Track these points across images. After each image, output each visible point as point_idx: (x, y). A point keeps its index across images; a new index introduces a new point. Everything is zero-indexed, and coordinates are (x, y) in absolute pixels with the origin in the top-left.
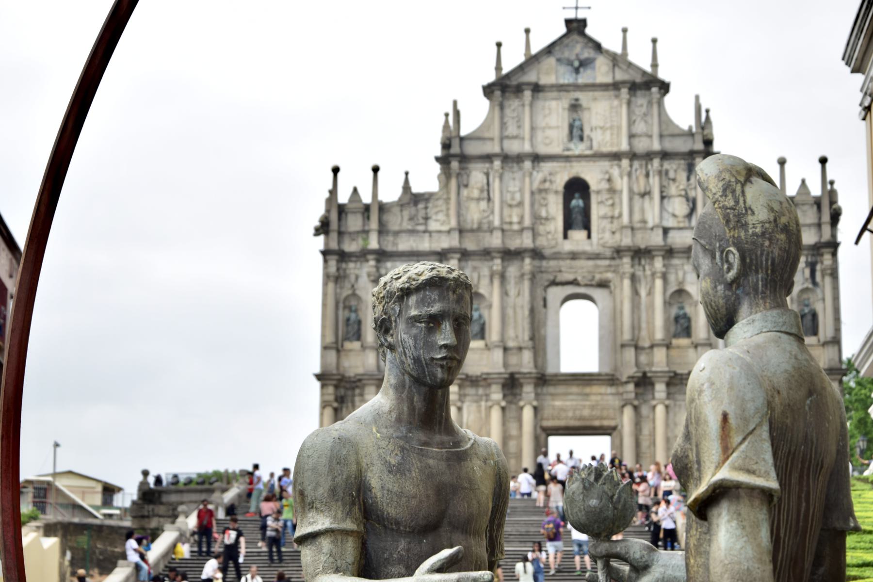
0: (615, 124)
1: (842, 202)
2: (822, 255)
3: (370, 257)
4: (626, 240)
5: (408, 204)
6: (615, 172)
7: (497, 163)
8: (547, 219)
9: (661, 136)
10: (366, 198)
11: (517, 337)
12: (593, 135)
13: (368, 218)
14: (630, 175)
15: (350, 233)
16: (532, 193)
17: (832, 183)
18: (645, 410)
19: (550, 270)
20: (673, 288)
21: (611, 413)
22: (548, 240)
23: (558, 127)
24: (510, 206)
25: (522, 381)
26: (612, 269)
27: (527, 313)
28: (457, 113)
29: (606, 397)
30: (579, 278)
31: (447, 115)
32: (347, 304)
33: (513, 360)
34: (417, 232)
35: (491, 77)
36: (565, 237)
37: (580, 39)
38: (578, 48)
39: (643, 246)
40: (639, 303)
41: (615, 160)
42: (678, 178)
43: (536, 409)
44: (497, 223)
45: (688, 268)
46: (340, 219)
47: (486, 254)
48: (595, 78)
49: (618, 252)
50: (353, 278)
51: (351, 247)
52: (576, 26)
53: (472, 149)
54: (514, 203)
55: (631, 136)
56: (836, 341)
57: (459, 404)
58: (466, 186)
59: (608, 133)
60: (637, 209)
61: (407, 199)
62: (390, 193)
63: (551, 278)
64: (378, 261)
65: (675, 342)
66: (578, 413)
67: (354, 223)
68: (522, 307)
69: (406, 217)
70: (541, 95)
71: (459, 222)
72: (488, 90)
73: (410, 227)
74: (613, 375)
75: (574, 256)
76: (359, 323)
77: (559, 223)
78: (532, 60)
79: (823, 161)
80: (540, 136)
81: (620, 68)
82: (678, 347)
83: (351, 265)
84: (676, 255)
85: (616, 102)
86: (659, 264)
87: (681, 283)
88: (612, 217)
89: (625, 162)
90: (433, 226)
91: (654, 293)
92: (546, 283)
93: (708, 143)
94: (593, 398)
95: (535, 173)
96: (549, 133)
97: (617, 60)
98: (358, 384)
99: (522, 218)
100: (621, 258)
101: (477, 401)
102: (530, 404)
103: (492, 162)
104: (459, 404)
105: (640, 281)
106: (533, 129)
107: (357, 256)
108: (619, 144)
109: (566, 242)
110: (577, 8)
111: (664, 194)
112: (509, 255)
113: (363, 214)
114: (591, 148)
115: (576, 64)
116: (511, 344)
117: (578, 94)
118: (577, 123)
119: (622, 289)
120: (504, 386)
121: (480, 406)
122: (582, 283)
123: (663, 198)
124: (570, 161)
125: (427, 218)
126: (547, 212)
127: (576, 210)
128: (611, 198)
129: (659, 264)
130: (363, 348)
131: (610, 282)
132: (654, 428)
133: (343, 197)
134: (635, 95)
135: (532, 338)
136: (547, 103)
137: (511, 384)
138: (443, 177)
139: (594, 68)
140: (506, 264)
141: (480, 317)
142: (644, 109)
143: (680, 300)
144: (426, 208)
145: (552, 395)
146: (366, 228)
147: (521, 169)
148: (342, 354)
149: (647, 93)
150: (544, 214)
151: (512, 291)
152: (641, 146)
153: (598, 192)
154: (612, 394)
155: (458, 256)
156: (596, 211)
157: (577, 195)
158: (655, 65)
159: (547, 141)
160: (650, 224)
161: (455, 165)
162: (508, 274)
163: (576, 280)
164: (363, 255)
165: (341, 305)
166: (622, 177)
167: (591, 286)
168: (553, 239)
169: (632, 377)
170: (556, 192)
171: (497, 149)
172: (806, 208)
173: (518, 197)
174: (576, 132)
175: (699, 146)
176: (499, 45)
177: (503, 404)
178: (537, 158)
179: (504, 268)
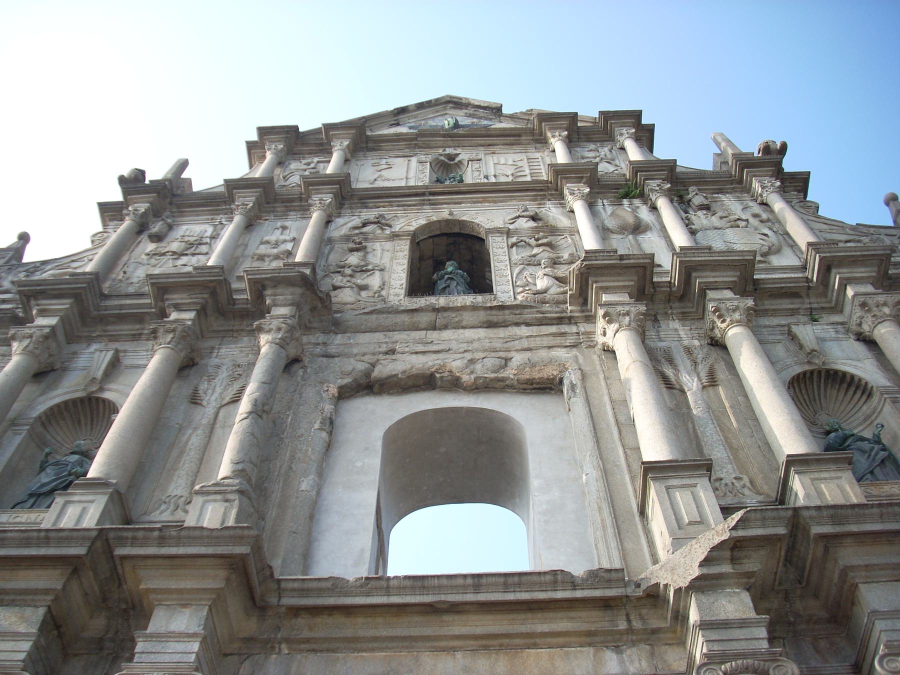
8: (362, 270)
19: (355, 351)
26: (570, 340)
58: (158, 238)
63: (361, 366)
85: (538, 155)
95: (340, 221)
105: (671, 361)
122: (466, 378)
136: (384, 161)
153: (509, 233)
162: (214, 361)
170: (395, 236)
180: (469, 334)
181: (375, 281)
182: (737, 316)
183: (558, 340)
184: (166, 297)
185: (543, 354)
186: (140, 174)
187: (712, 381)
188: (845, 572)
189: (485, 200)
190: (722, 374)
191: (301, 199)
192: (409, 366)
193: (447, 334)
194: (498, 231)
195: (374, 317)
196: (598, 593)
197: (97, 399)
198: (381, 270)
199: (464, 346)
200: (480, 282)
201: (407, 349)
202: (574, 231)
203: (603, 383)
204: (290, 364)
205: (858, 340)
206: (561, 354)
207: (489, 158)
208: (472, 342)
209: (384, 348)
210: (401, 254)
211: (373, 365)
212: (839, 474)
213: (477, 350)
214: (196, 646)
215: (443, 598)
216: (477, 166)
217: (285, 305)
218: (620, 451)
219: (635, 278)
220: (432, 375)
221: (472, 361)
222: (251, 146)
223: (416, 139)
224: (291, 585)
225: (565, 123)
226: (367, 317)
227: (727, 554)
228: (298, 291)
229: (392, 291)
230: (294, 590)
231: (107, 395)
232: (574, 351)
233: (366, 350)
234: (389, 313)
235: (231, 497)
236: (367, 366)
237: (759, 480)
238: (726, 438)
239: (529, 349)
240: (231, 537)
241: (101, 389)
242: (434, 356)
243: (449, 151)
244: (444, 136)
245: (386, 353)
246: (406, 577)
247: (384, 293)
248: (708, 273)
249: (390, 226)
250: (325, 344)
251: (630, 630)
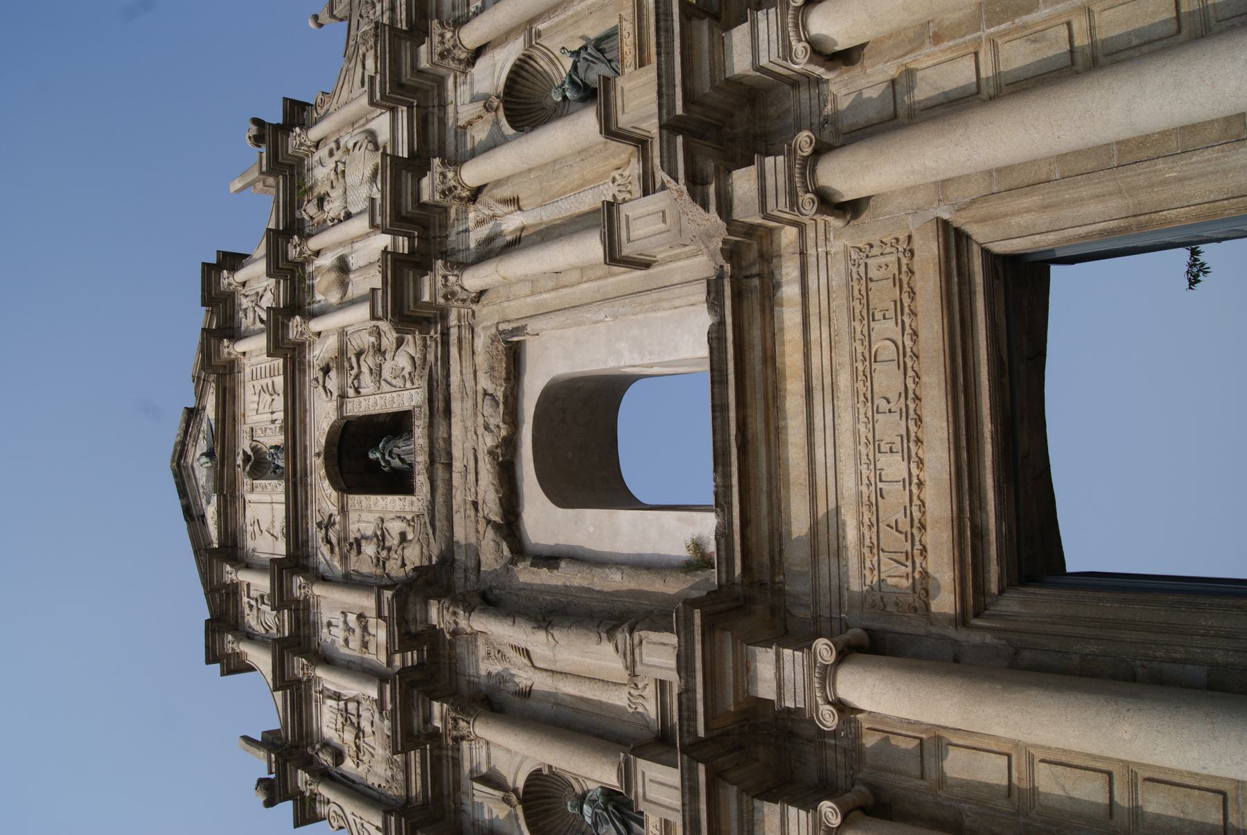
21: (882, 265)
25: (730, 703)
26: (466, 334)
30: (489, 441)
58: (339, 756)
63: (490, 533)
66: (890, 427)
85: (248, 370)
95: (323, 567)
102: (827, 675)
122: (504, 433)
136: (249, 529)
153: (343, 396)
163: (491, 453)
170: (343, 511)
173: (352, 619)
180: (456, 431)
181: (395, 527)
182: (450, 175)
183: (466, 346)
184: (416, 733)
185: (480, 359)
186: (264, 784)
187: (514, 202)
188: (714, 88)
189: (303, 422)
190: (506, 192)
191: (297, 610)
192: (491, 487)
193: (457, 452)
194: (340, 407)
195: (438, 524)
196: (728, 303)
197: (524, 792)
198: (382, 521)
199: (471, 434)
200: (398, 424)
201: (473, 490)
202: (343, 333)
203: (513, 303)
204: (491, 600)
205: (473, 64)
206: (481, 342)
207: (248, 420)
208: (466, 428)
209: (472, 512)
210: (364, 503)
211: (489, 522)
212: (619, 89)
213: (475, 422)
214: (787, 652)
215: (733, 438)
216: (259, 432)
217: (426, 612)
218: (584, 286)
219: (406, 270)
220: (500, 465)
221: (487, 428)
222: (228, 671)
223: (225, 496)
224: (724, 575)
226: (437, 534)
227: (699, 189)
228: (411, 599)
229: (407, 509)
230: (727, 572)
231: (520, 784)
232: (478, 330)
233: (473, 530)
234: (433, 508)
235: (636, 641)
236: (490, 527)
237: (616, 162)
238: (572, 190)
239: (475, 372)
240: (686, 628)
241: (515, 791)
242: (480, 463)
243: (239, 461)
244: (222, 466)
245: (477, 510)
246: (715, 471)
247: (409, 517)
248: (403, 200)
249: (331, 515)
250: (465, 571)
251: (759, 275)
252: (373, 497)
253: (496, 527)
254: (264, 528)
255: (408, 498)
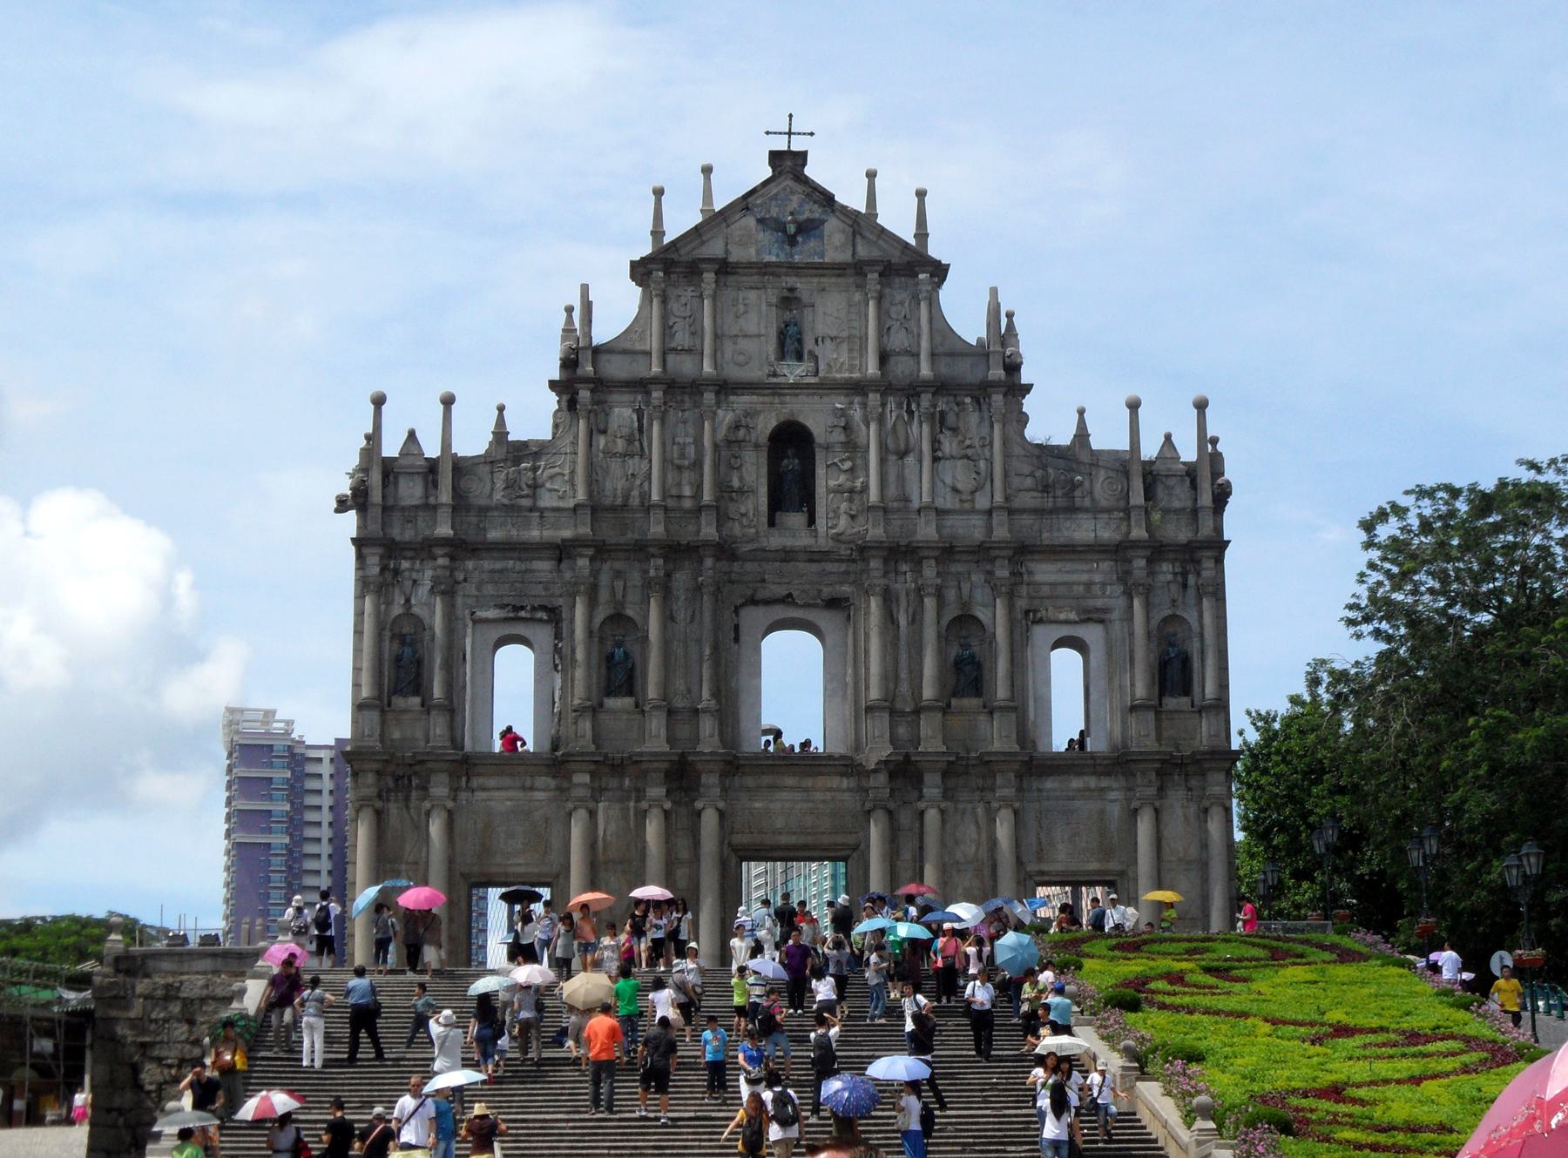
0: (856, 332)
1: (1230, 473)
2: (1199, 562)
3: (439, 551)
4: (875, 531)
5: (505, 460)
6: (857, 414)
7: (657, 394)
9: (933, 355)
10: (432, 449)
11: (689, 691)
12: (818, 351)
13: (435, 485)
14: (881, 420)
15: (403, 509)
16: (716, 446)
17: (1214, 441)
18: (905, 818)
20: (951, 612)
22: (743, 526)
23: (759, 336)
24: (679, 468)
25: (699, 767)
27: (707, 652)
28: (587, 307)
29: (839, 796)
30: (795, 594)
31: (570, 310)
32: (397, 631)
33: (683, 731)
34: (520, 508)
35: (646, 249)
36: (772, 523)
37: (799, 188)
38: (795, 202)
39: (903, 542)
40: (897, 637)
41: (858, 394)
42: (961, 425)
43: (722, 814)
44: (655, 497)
45: (978, 578)
46: (385, 486)
47: (640, 550)
48: (822, 256)
49: (863, 550)
50: (408, 583)
51: (401, 532)
52: (788, 164)
53: (616, 368)
54: (686, 463)
55: (884, 358)
56: (1221, 705)
57: (591, 805)
58: (604, 432)
59: (845, 346)
60: (892, 478)
61: (501, 453)
62: (472, 441)
63: (749, 592)
64: (452, 558)
65: (954, 702)
67: (410, 492)
68: (699, 641)
69: (500, 485)
70: (731, 279)
71: (590, 494)
72: (641, 270)
73: (506, 501)
74: (850, 758)
75: (787, 555)
76: (419, 663)
77: (763, 500)
78: (715, 221)
79: (1201, 406)
80: (728, 348)
81: (863, 237)
82: (961, 712)
83: (405, 564)
84: (957, 557)
85: (858, 297)
86: (930, 571)
87: (965, 605)
88: (852, 491)
89: (874, 398)
90: (546, 501)
91: (922, 619)
92: (739, 601)
93: (1013, 367)
94: (819, 796)
95: (720, 413)
96: (744, 344)
97: (862, 224)
98: (417, 768)
99: (699, 487)
100: (866, 560)
101: (622, 800)
103: (648, 393)
104: (591, 805)
106: (717, 337)
107: (414, 550)
108: (863, 367)
109: (774, 531)
110: (790, 133)
111: (940, 454)
112: (677, 552)
113: (425, 476)
114: (816, 373)
115: (792, 229)
116: (679, 703)
117: (791, 281)
118: (792, 330)
119: (867, 613)
120: (668, 776)
121: (625, 810)
123: (935, 459)
124: (780, 395)
125: (535, 486)
126: (741, 479)
127: (790, 476)
128: (848, 459)
129: (930, 571)
130: (427, 707)
131: (847, 599)
132: (921, 848)
133: (391, 447)
134: (890, 285)
135: (716, 694)
136: (741, 295)
137: (681, 775)
138: (566, 413)
139: (821, 237)
140: (671, 566)
141: (626, 654)
142: (905, 310)
143: (964, 633)
144: (535, 469)
145: (748, 790)
146: (432, 500)
147: (697, 405)
148: (390, 716)
149: (911, 281)
150: (736, 483)
151: (682, 615)
152: (901, 368)
153: (827, 448)
154: (849, 790)
155: (590, 552)
156: (826, 480)
157: (790, 452)
158: (922, 235)
159: (741, 359)
160: (916, 504)
161: (584, 395)
162: (675, 584)
163: (790, 595)
164: (425, 548)
165: (388, 634)
166: (868, 427)
167: (815, 606)
168: (749, 527)
169: (886, 762)
170: (757, 446)
171: (656, 369)
172: (1172, 482)
174: (790, 343)
175: (997, 373)
176: (659, 193)
177: (668, 805)
178: (725, 388)
179: (668, 575)
180: (801, 565)
194: (820, 446)
222: (634, 266)
225: (880, 268)
252: (764, 481)
253: (753, 596)
254: (741, 321)
255: (765, 520)
